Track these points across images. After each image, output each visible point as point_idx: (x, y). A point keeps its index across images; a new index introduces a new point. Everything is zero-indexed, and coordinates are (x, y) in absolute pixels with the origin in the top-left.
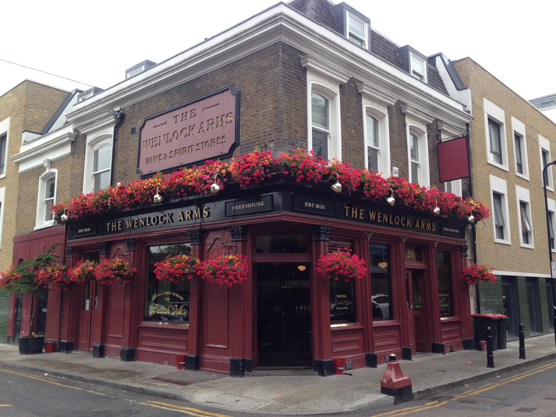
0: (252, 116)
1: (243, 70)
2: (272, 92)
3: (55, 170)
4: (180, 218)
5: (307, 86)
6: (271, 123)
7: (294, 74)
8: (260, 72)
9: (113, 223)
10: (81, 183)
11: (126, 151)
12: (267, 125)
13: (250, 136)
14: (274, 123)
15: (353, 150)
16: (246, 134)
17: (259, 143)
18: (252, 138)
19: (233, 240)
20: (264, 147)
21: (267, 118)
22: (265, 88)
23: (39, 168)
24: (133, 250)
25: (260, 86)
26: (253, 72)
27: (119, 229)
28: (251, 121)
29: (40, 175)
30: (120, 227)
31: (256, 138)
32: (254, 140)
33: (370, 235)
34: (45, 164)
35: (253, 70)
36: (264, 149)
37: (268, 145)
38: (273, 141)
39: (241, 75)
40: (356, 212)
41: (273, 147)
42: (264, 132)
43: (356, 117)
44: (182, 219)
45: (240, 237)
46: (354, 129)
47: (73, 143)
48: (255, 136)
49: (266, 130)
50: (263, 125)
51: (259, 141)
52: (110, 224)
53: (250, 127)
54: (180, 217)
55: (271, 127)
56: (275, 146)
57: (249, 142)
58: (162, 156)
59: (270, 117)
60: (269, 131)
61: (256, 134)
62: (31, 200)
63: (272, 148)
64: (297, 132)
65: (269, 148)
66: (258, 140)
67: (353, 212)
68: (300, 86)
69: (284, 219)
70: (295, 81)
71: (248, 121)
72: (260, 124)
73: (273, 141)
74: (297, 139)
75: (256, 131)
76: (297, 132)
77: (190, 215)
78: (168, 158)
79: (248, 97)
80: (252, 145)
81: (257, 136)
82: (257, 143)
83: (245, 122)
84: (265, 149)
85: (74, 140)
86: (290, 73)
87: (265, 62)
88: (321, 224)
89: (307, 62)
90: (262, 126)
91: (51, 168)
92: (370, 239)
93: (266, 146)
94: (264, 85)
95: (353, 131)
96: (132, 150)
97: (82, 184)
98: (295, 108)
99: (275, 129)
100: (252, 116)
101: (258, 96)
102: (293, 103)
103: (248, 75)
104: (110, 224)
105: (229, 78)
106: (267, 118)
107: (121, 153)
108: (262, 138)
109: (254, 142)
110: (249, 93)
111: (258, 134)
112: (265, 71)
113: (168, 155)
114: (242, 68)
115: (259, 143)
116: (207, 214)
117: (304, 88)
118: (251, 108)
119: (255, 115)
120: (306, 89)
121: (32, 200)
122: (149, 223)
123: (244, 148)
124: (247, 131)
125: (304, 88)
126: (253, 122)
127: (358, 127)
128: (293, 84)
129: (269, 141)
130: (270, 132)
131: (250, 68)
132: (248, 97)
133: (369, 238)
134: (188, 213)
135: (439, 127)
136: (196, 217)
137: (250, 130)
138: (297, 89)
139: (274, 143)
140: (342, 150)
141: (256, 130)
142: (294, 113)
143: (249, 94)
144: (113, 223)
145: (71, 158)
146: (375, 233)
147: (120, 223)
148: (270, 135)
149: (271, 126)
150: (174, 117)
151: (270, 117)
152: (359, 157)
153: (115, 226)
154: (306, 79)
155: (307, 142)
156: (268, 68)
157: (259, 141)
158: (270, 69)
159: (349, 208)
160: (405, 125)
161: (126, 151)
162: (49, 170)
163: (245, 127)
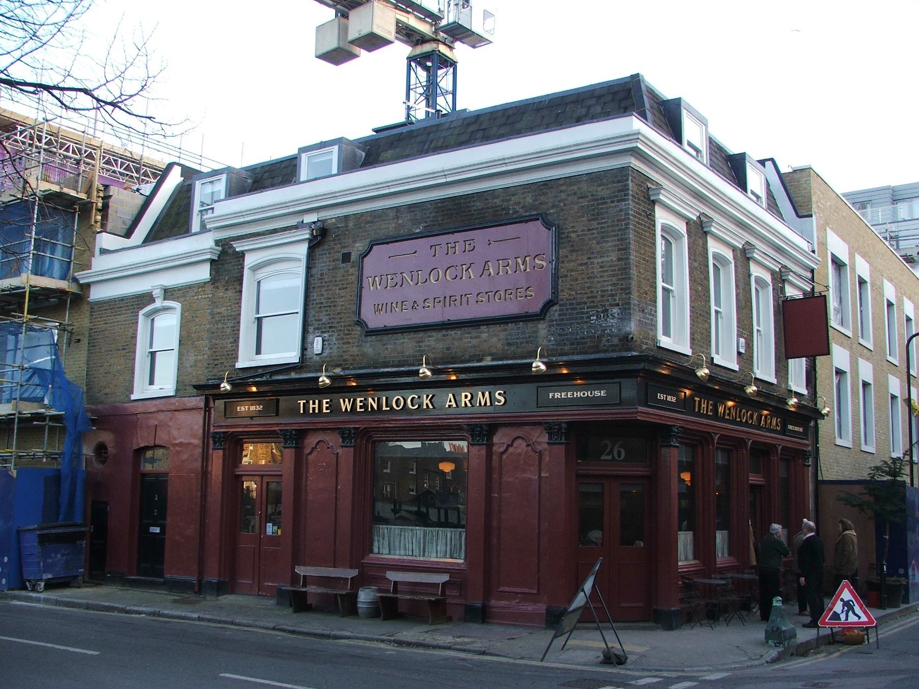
0: (581, 265)
1: (563, 196)
2: (615, 236)
3: (177, 305)
4: (450, 404)
5: (656, 226)
6: (614, 279)
7: (644, 211)
8: (595, 203)
9: (311, 402)
10: (233, 331)
11: (330, 288)
12: (608, 281)
13: (576, 293)
14: (619, 280)
15: (700, 315)
16: (569, 289)
17: (592, 304)
18: (580, 296)
19: (551, 441)
20: (602, 312)
21: (607, 271)
22: (602, 228)
23: (137, 297)
24: (354, 446)
25: (595, 223)
26: (581, 200)
27: (325, 411)
28: (578, 271)
29: (142, 308)
30: (327, 408)
31: (588, 298)
32: (585, 300)
33: (717, 437)
34: (157, 293)
35: (581, 198)
36: (602, 315)
37: (610, 310)
38: (618, 305)
39: (559, 201)
40: (705, 406)
41: (618, 314)
42: (604, 291)
43: (702, 267)
44: (454, 405)
45: (563, 438)
46: (701, 285)
47: (212, 262)
48: (586, 293)
49: (606, 289)
50: (599, 280)
51: (593, 302)
52: (305, 401)
53: (577, 280)
54: (450, 401)
55: (614, 285)
56: (622, 313)
57: (575, 301)
58: (409, 304)
59: (612, 271)
60: (611, 290)
61: (588, 291)
62: (121, 348)
63: (616, 315)
64: (646, 294)
65: (611, 315)
66: (591, 300)
67: (703, 406)
68: (649, 228)
69: (639, 418)
70: (644, 221)
71: (572, 271)
72: (594, 278)
73: (618, 305)
74: (646, 304)
75: (588, 288)
76: (646, 294)
77: (470, 401)
78: (420, 308)
79: (573, 235)
80: (582, 306)
81: (590, 295)
82: (588, 305)
83: (567, 271)
84: (604, 316)
85: (216, 258)
86: (639, 209)
87: (602, 190)
88: (673, 424)
89: (659, 194)
90: (598, 282)
91: (165, 299)
92: (717, 443)
93: (607, 311)
94: (602, 223)
95: (700, 288)
96: (344, 289)
97: (235, 332)
98: (644, 260)
99: (622, 289)
100: (581, 265)
101: (591, 237)
102: (642, 252)
103: (572, 203)
104: (305, 401)
105: (536, 203)
106: (607, 271)
107: (321, 291)
108: (599, 298)
109: (585, 303)
110: (575, 230)
111: (591, 292)
112: (603, 204)
113: (421, 305)
114: (561, 191)
115: (592, 304)
116: (503, 400)
117: (652, 230)
118: (580, 253)
119: (586, 264)
120: (655, 231)
121: (123, 349)
122: (386, 407)
123: (567, 310)
124: (572, 285)
125: (652, 230)
126: (582, 273)
127: (705, 282)
128: (642, 224)
129: (611, 305)
130: (613, 292)
131: (575, 194)
132: (573, 235)
133: (716, 441)
134: (466, 397)
135: (784, 276)
136: (483, 404)
137: (578, 284)
138: (646, 231)
139: (620, 309)
140: (691, 316)
141: (588, 285)
142: (643, 266)
143: (574, 232)
144: (311, 402)
145: (209, 288)
146: (722, 435)
147: (327, 403)
148: (612, 295)
149: (614, 284)
150: (431, 246)
151: (612, 271)
152: (706, 325)
153: (317, 406)
154: (654, 216)
155: (656, 307)
156: (609, 201)
157: (593, 302)
158: (612, 202)
159: (699, 399)
160: (749, 276)
161: (330, 288)
162: (162, 303)
163: (568, 279)
